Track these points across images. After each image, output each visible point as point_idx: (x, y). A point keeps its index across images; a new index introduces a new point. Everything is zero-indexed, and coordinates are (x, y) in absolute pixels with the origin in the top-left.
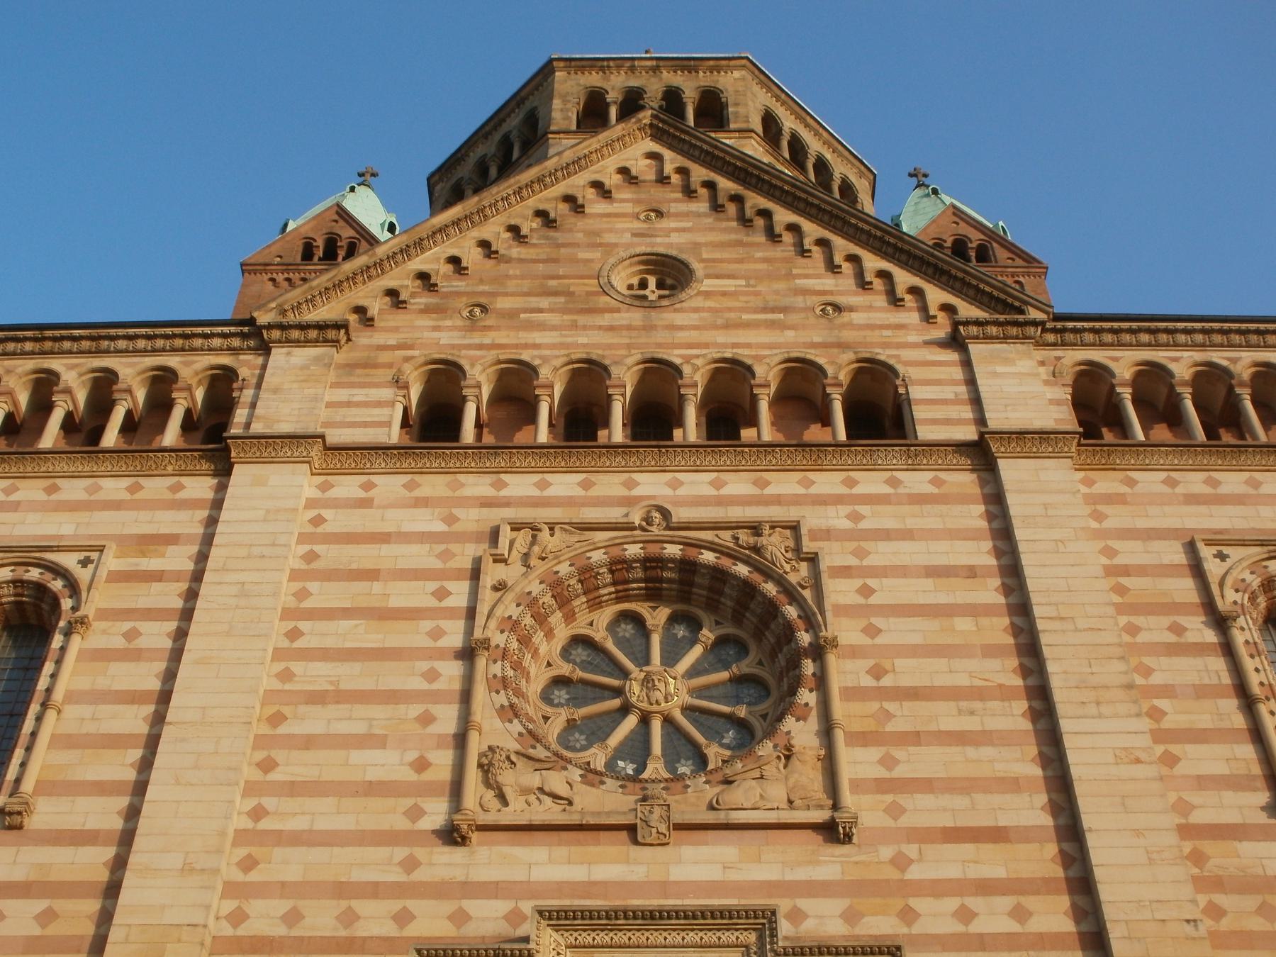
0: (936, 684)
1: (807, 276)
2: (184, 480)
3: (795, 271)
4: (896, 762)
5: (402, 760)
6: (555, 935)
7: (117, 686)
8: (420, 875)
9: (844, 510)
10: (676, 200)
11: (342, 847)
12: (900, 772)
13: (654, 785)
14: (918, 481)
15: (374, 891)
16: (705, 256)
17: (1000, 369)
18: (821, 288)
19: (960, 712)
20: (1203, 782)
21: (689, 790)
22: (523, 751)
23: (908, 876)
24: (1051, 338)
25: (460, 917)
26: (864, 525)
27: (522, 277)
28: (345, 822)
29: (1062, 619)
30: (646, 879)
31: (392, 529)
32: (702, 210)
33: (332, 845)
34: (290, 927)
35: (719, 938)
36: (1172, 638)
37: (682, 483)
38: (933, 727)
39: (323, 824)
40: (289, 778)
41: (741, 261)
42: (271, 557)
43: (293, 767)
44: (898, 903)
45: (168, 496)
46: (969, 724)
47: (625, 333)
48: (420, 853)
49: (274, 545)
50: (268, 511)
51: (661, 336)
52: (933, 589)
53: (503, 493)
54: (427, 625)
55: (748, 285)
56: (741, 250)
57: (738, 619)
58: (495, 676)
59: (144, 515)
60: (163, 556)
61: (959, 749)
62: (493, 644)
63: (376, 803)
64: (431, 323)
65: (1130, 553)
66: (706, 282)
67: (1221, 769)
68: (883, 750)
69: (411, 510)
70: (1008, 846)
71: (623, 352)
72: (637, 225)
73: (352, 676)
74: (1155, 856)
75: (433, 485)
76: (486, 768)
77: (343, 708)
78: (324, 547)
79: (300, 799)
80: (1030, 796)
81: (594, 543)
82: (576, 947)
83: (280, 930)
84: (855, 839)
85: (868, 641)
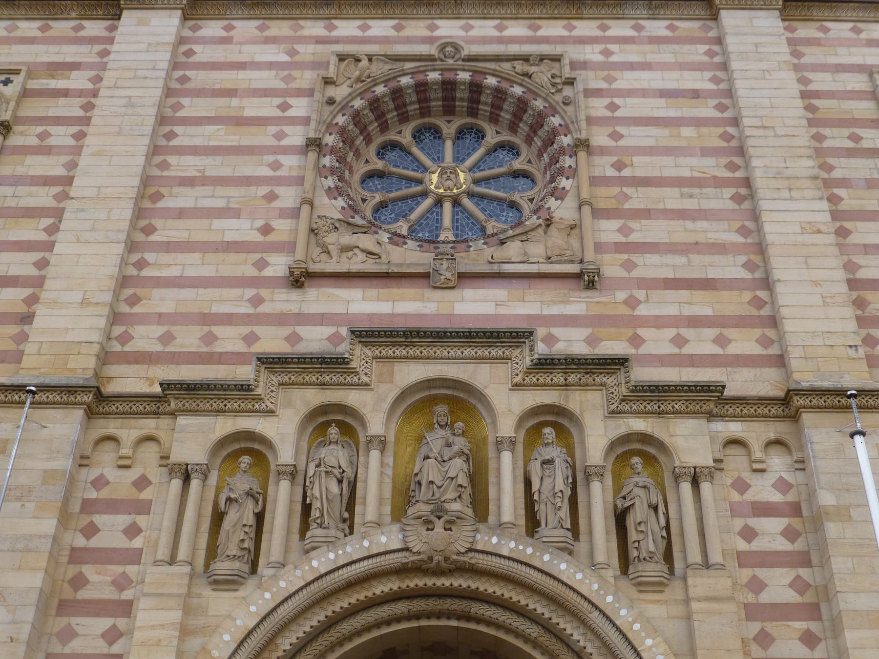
0: (665, 175)
2: (84, 23)
4: (632, 231)
5: (252, 226)
6: (366, 350)
7: (32, 172)
8: (264, 308)
11: (205, 288)
12: (634, 238)
13: (445, 245)
15: (229, 319)
19: (682, 196)
21: (471, 249)
22: (345, 220)
23: (637, 313)
25: (294, 339)
26: (614, 59)
28: (207, 271)
29: (765, 127)
30: (436, 313)
33: (198, 287)
34: (165, 345)
35: (490, 353)
36: (851, 144)
37: (472, 27)
38: (661, 206)
39: (190, 272)
40: (166, 239)
42: (152, 78)
44: (629, 332)
45: (72, 34)
48: (264, 293)
49: (154, 69)
50: (150, 44)
52: (665, 106)
53: (335, 33)
54: (273, 129)
57: (513, 128)
58: (324, 166)
59: (53, 48)
60: (68, 78)
61: (681, 222)
62: (324, 143)
63: (233, 257)
65: (821, 81)
68: (622, 222)
69: (263, 46)
70: (716, 292)
73: (214, 166)
74: (828, 300)
75: (280, 28)
76: (316, 231)
77: (207, 190)
78: (195, 72)
79: (173, 254)
80: (734, 257)
81: (403, 70)
82: (380, 358)
83: (158, 348)
84: (597, 286)
85: (613, 143)
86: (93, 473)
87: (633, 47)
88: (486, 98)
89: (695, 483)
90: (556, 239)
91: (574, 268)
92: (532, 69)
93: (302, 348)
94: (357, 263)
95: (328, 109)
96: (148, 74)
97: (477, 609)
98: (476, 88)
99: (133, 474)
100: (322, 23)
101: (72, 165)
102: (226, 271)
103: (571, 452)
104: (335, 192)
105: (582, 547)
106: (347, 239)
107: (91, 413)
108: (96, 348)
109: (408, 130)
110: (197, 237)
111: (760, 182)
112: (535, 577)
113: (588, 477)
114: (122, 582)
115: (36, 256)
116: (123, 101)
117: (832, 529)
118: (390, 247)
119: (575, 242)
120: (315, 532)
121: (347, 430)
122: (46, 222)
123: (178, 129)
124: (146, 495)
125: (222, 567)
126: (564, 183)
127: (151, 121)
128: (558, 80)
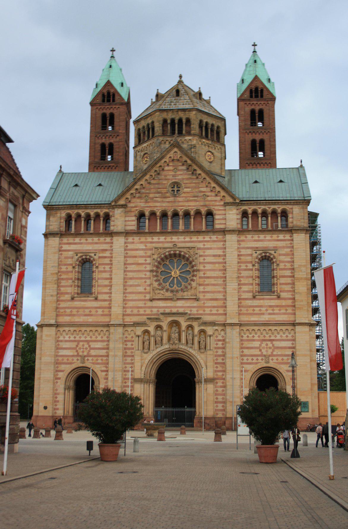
1: (202, 187)
3: (200, 186)
8: (146, 305)
9: (203, 243)
12: (205, 290)
14: (214, 238)
15: (141, 307)
16: (185, 182)
17: (231, 212)
20: (244, 292)
25: (152, 311)
26: (205, 247)
27: (154, 188)
28: (136, 298)
39: (134, 298)
41: (190, 183)
43: (129, 290)
46: (215, 282)
48: (146, 302)
51: (177, 204)
54: (144, 266)
56: (191, 180)
59: (102, 245)
63: (140, 295)
65: (243, 252)
67: (246, 290)
72: (173, 173)
73: (135, 275)
75: (143, 239)
86: (125, 336)
87: (209, 243)
88: (182, 257)
89: (210, 336)
90: (193, 291)
91: (195, 297)
92: (190, 251)
93: (153, 313)
95: (154, 261)
96: (121, 254)
97: (179, 354)
99: (131, 336)
101: (111, 275)
103: (193, 332)
104: (156, 281)
105: (194, 346)
106: (159, 292)
107: (124, 327)
108: (122, 315)
109: (168, 261)
110: (134, 291)
112: (187, 352)
113: (195, 336)
114: (132, 352)
115: (109, 295)
117: (227, 345)
119: (195, 291)
122: (109, 288)
123: (128, 266)
124: (133, 339)
125: (145, 351)
126: (195, 278)
127: (123, 266)
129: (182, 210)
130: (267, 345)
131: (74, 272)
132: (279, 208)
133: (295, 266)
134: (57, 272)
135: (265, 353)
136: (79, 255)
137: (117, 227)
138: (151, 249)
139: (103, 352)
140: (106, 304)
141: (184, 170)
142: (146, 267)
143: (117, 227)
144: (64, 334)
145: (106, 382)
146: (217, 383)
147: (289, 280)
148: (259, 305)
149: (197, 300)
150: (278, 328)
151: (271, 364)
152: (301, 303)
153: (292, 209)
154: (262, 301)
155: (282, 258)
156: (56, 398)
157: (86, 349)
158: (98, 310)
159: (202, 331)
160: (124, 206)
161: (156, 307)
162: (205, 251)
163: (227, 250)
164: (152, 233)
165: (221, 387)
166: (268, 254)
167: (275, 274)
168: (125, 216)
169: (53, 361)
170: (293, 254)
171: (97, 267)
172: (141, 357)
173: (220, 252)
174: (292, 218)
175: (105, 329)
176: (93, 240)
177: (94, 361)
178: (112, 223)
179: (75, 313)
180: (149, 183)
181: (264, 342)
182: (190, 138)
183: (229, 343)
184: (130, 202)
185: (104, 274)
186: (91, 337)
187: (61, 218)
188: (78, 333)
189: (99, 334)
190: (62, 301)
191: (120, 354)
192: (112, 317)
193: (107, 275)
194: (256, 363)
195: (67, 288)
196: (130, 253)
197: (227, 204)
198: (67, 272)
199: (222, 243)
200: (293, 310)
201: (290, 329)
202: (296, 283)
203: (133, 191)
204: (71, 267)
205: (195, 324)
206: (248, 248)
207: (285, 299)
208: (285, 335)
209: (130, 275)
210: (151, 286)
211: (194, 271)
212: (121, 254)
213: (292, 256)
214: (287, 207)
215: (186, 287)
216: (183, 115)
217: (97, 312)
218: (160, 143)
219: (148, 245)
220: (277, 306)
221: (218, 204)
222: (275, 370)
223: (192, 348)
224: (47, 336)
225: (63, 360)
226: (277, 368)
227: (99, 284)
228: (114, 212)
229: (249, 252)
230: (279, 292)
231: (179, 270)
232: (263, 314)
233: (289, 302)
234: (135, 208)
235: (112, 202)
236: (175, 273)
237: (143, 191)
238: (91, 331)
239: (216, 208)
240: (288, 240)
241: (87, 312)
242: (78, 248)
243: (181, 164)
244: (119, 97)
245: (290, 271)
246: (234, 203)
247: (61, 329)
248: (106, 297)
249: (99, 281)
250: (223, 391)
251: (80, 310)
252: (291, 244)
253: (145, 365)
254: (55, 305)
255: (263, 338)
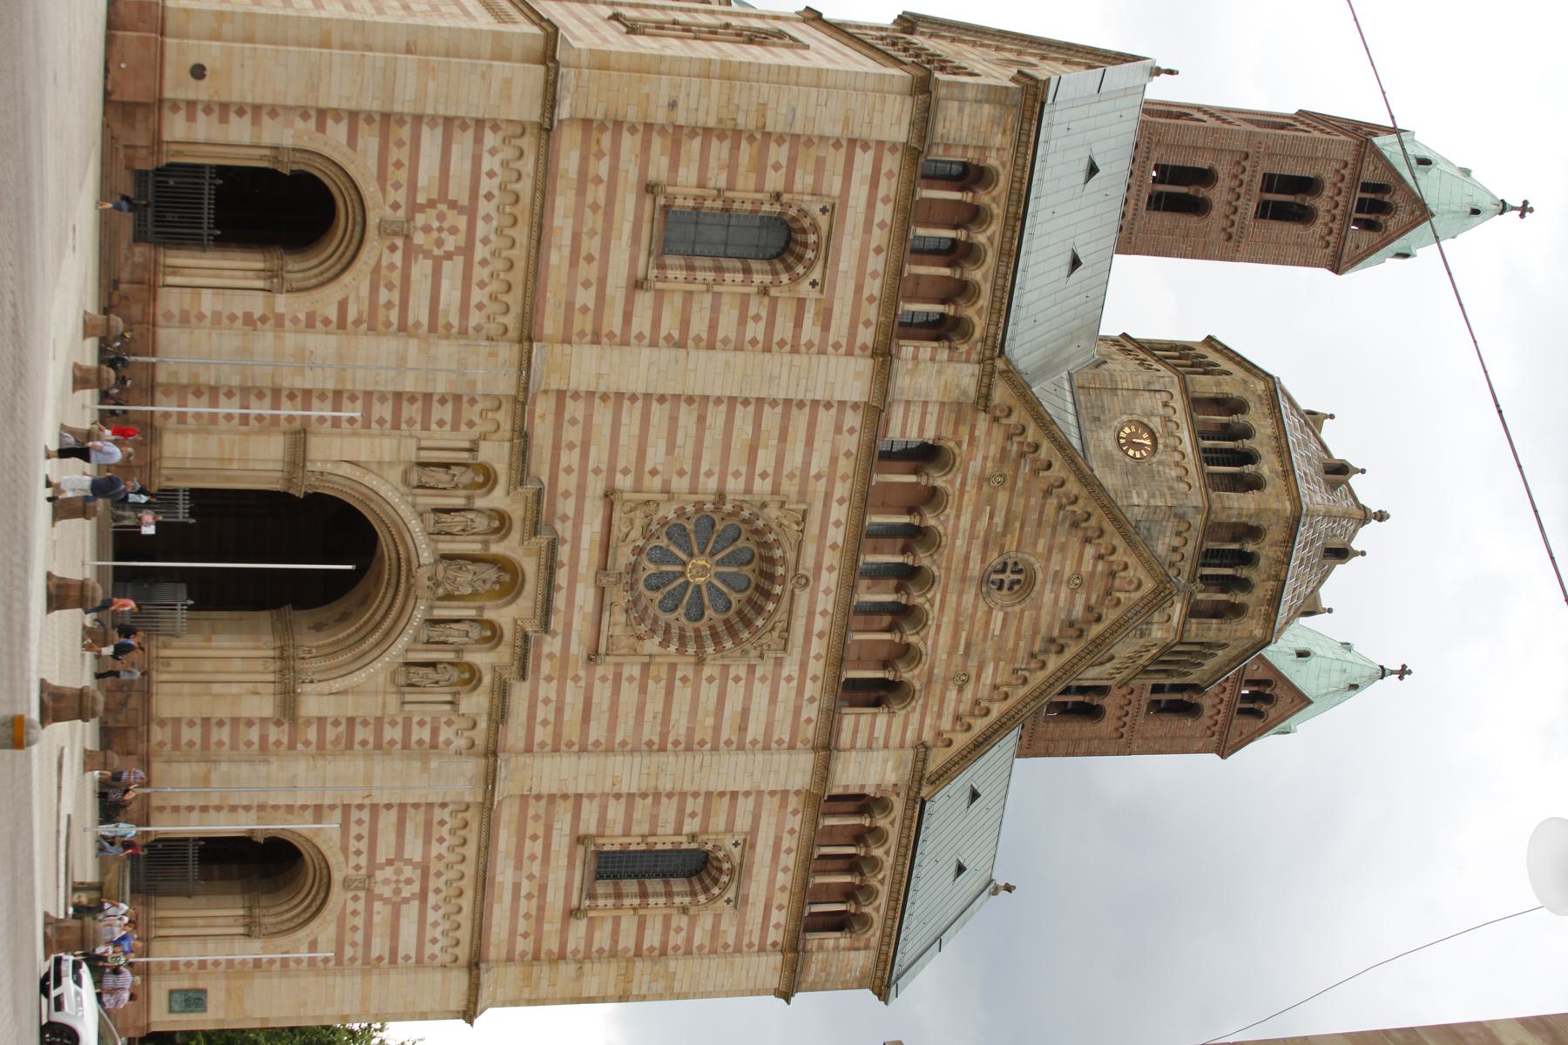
1: (996, 669)
3: (1002, 664)
8: (591, 477)
9: (795, 674)
10: (1088, 599)
12: (625, 684)
14: (810, 711)
15: (585, 455)
16: (1027, 613)
17: (890, 764)
18: (983, 675)
22: (655, 522)
24: (912, 794)
25: (567, 494)
26: (783, 683)
27: (1026, 507)
28: (623, 439)
31: (816, 445)
32: (1074, 613)
39: (623, 430)
41: (1018, 633)
44: (555, 675)
46: (648, 716)
47: (961, 566)
48: (603, 476)
51: (953, 586)
53: (834, 505)
54: (743, 469)
55: (993, 636)
57: (739, 612)
59: (848, 310)
60: (814, 324)
64: (991, 454)
65: (745, 806)
66: (1001, 615)
67: (610, 815)
71: (944, 564)
72: (1067, 573)
73: (713, 436)
75: (845, 466)
87: (793, 694)
88: (760, 600)
89: (450, 703)
90: (625, 642)
91: (602, 649)
92: (775, 634)
93: (560, 500)
94: (619, 528)
96: (802, 388)
97: (391, 591)
98: (767, 595)
99: (476, 419)
100: (846, 494)
102: (622, 452)
104: (681, 512)
105: (420, 646)
110: (652, 432)
111: (657, 759)
113: (457, 651)
114: (411, 422)
115: (647, 332)
116: (776, 373)
118: (631, 547)
120: (431, 517)
121: (496, 531)
124: (463, 428)
126: (673, 648)
128: (765, 647)
129: (927, 606)
130: (409, 882)
131: (759, 196)
132: (877, 909)
133: (672, 965)
134: (768, 129)
135: (379, 875)
136: (823, 221)
137: (908, 372)
138: (803, 495)
139: (419, 311)
140: (614, 322)
141: (1070, 611)
142: (737, 474)
143: (907, 373)
144: (508, 153)
145: (295, 320)
146: (278, 723)
147: (627, 941)
148: (553, 855)
149: (593, 657)
150: (465, 918)
151: (337, 895)
152: (544, 983)
153: (866, 948)
154: (564, 862)
155: (706, 922)
156: (241, 112)
157: (440, 243)
158: (593, 290)
159: (472, 677)
160: (983, 400)
161: (579, 511)
162: (768, 683)
163: (760, 757)
164: (865, 499)
165: (263, 739)
166: (725, 879)
167: (652, 901)
168: (942, 404)
169: (397, 108)
170: (713, 952)
171: (764, 291)
172: (391, 463)
173: (755, 729)
174: (836, 948)
175: (511, 321)
176: (874, 275)
177: (384, 271)
178: (926, 349)
179: (589, 200)
180: (1048, 493)
181: (419, 871)
182: (1175, 619)
183: (425, 769)
184: (996, 419)
185: (735, 314)
186: (484, 263)
187: (983, 149)
188: (508, 209)
189: (493, 298)
190: (646, 146)
191: (409, 386)
192: (558, 348)
193: (728, 324)
194: (344, 849)
195: (695, 166)
196: (800, 419)
197: (921, 756)
198: (760, 168)
199: (786, 738)
200: (523, 954)
201: (458, 951)
202: (614, 965)
203: (1032, 434)
204: (780, 187)
205: (503, 655)
206: (756, 818)
207: (564, 931)
208: (438, 936)
209: (716, 416)
210: (665, 496)
211: (699, 639)
212: (802, 388)
213: (706, 950)
214: (874, 935)
215: (642, 620)
216: (1261, 594)
217: (586, 285)
218: (1181, 517)
219: (821, 486)
220: (541, 908)
221: (928, 721)
222: (318, 902)
223: (415, 640)
224: (508, 82)
225: (400, 144)
226: (325, 913)
227: (696, 298)
228: (967, 361)
229: (743, 823)
230: (591, 914)
231: (710, 585)
232: (518, 866)
233: (551, 944)
234: (966, 439)
235: (1008, 362)
236: (701, 570)
237: (1026, 468)
238: (511, 266)
239: (915, 718)
240: (763, 937)
241: (592, 245)
242: (850, 213)
243: (1093, 601)
244: (1364, 246)
245: (657, 944)
246: (921, 778)
247: (528, 143)
248: (642, 322)
249: (708, 299)
250: (249, 744)
251: (600, 217)
252: (750, 945)
253: (357, 474)
254: (632, 115)
255: (433, 871)
